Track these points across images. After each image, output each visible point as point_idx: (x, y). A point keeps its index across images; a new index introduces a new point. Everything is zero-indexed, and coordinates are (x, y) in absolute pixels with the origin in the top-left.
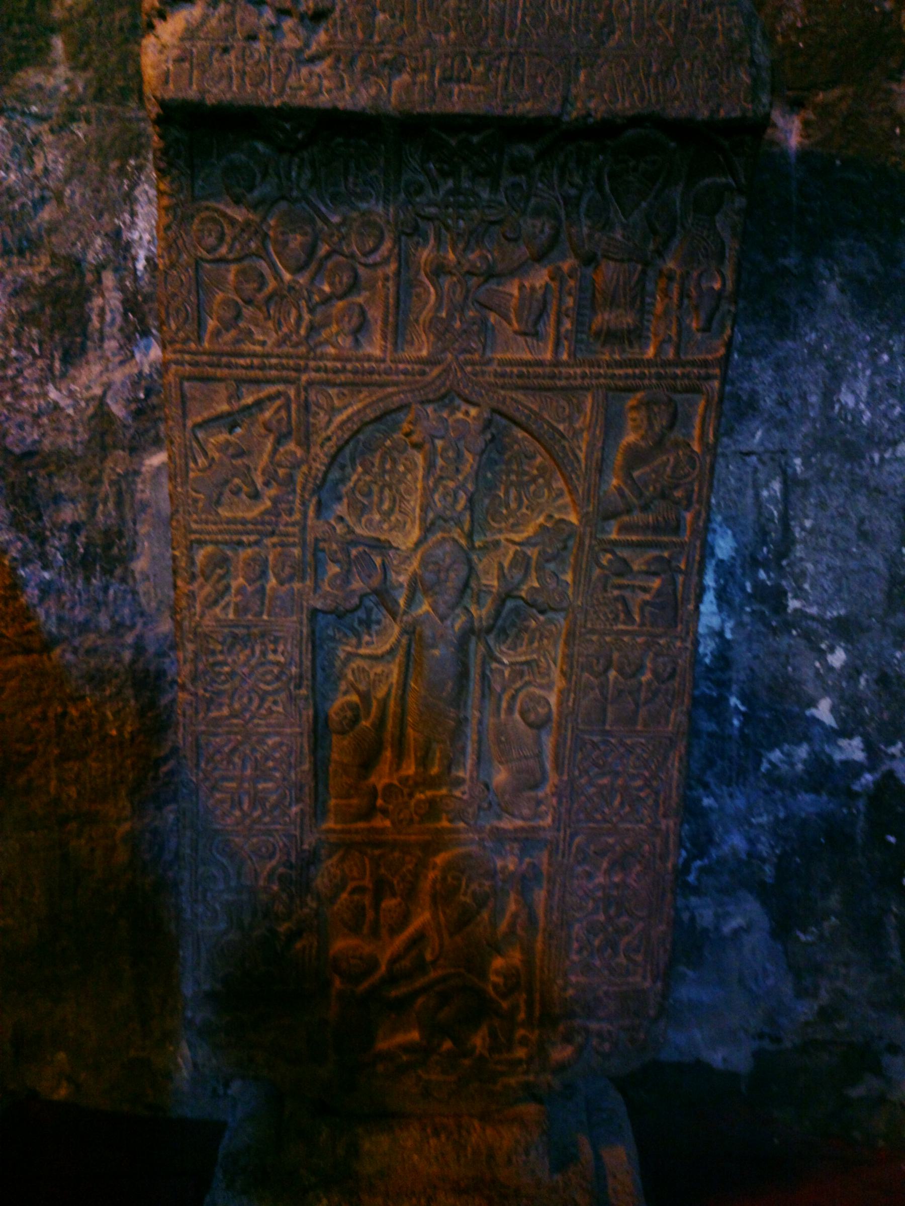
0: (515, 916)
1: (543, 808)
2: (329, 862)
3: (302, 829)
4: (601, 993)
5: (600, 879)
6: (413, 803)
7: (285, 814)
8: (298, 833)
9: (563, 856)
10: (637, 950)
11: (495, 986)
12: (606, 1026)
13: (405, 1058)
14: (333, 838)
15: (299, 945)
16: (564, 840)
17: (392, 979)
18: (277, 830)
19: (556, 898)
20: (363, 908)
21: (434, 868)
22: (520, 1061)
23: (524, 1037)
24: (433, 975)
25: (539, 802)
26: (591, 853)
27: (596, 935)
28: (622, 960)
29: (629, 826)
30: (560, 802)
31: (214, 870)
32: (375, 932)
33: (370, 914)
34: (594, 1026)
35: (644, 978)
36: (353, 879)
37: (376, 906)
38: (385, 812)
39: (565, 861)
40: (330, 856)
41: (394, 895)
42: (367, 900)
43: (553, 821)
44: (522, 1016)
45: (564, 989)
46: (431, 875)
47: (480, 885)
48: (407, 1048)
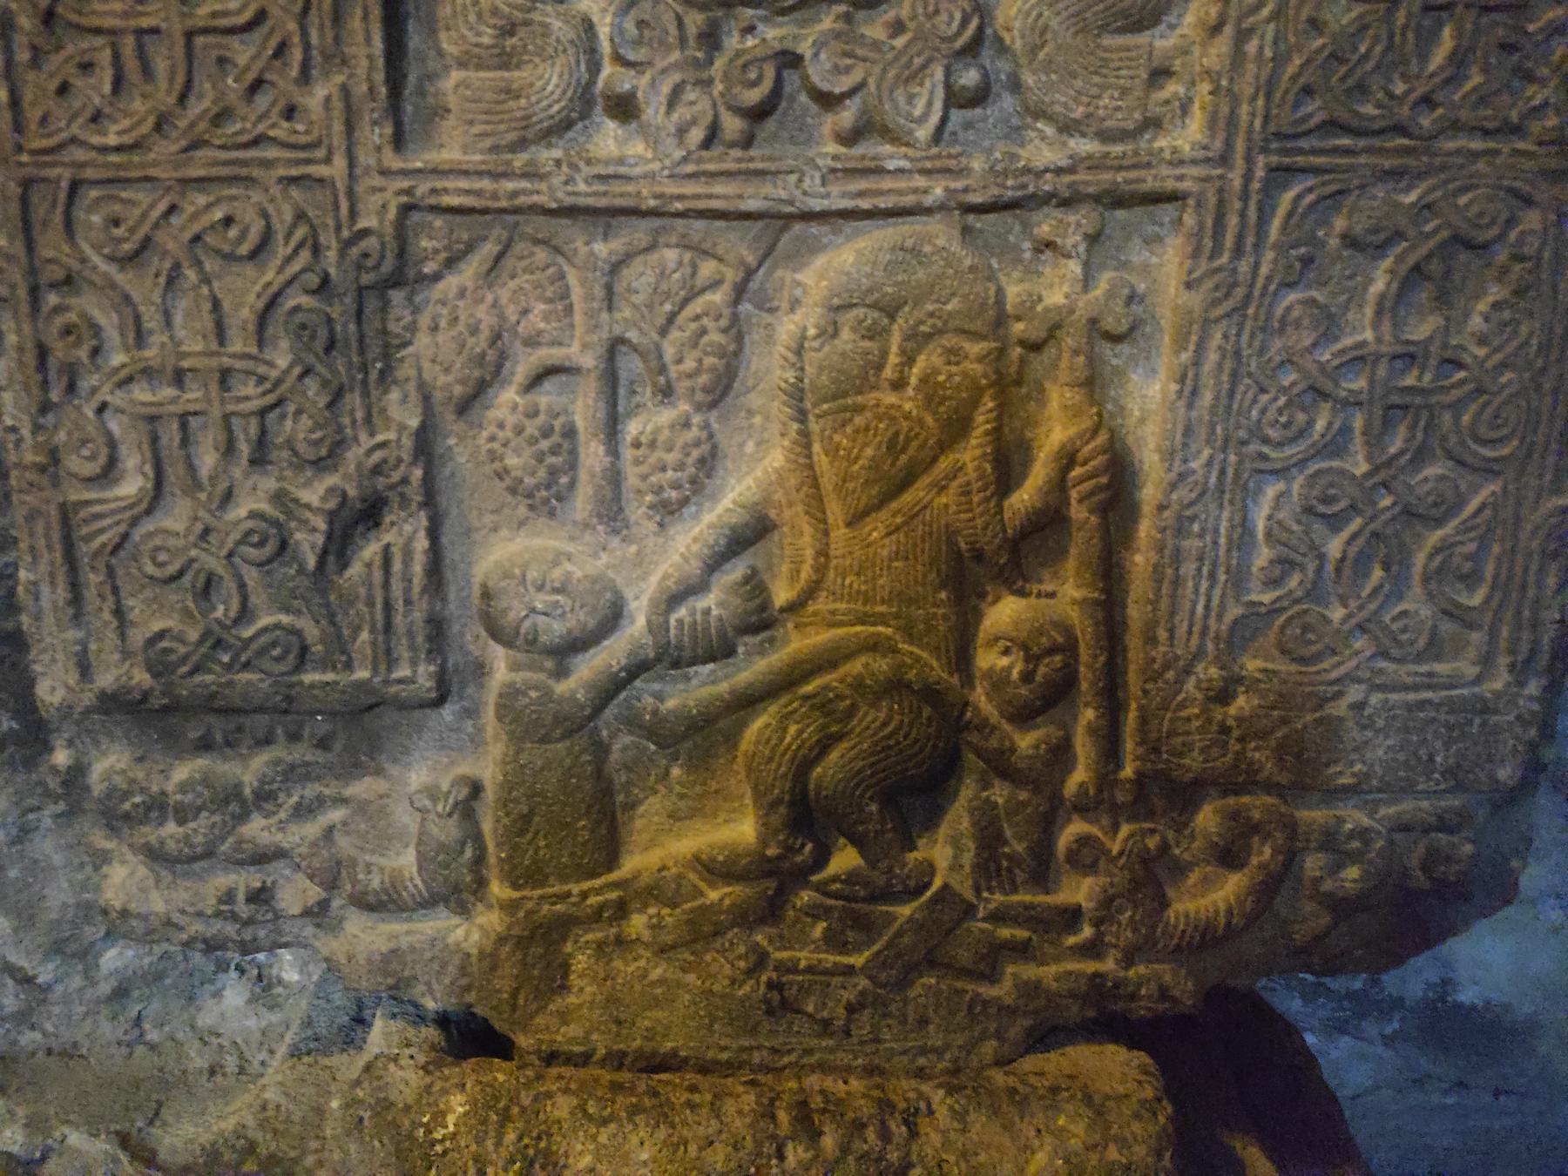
0: (1068, 458)
1: (1173, 88)
2: (452, 282)
3: (352, 163)
4: (1340, 708)
5: (1362, 331)
6: (720, 63)
7: (290, 113)
8: (338, 167)
9: (1238, 251)
10: (1470, 580)
11: (998, 682)
12: (1354, 817)
13: (713, 895)
14: (455, 193)
15: (370, 551)
16: (1245, 196)
17: (669, 658)
18: (267, 164)
19: (1207, 397)
20: (570, 432)
21: (795, 304)
22: (1071, 917)
23: (1084, 841)
24: (797, 643)
25: (1160, 74)
26: (1334, 242)
27: (1335, 523)
28: (1416, 603)
29: (1477, 145)
30: (1237, 58)
31: (89, 304)
32: (611, 512)
33: (593, 454)
34: (1313, 816)
35: (1486, 661)
36: (532, 342)
37: (612, 428)
38: (624, 108)
39: (1244, 266)
40: (451, 263)
41: (666, 393)
42: (583, 407)
43: (1212, 124)
44: (1079, 776)
45: (1223, 696)
46: (786, 328)
47: (954, 355)
48: (715, 869)
